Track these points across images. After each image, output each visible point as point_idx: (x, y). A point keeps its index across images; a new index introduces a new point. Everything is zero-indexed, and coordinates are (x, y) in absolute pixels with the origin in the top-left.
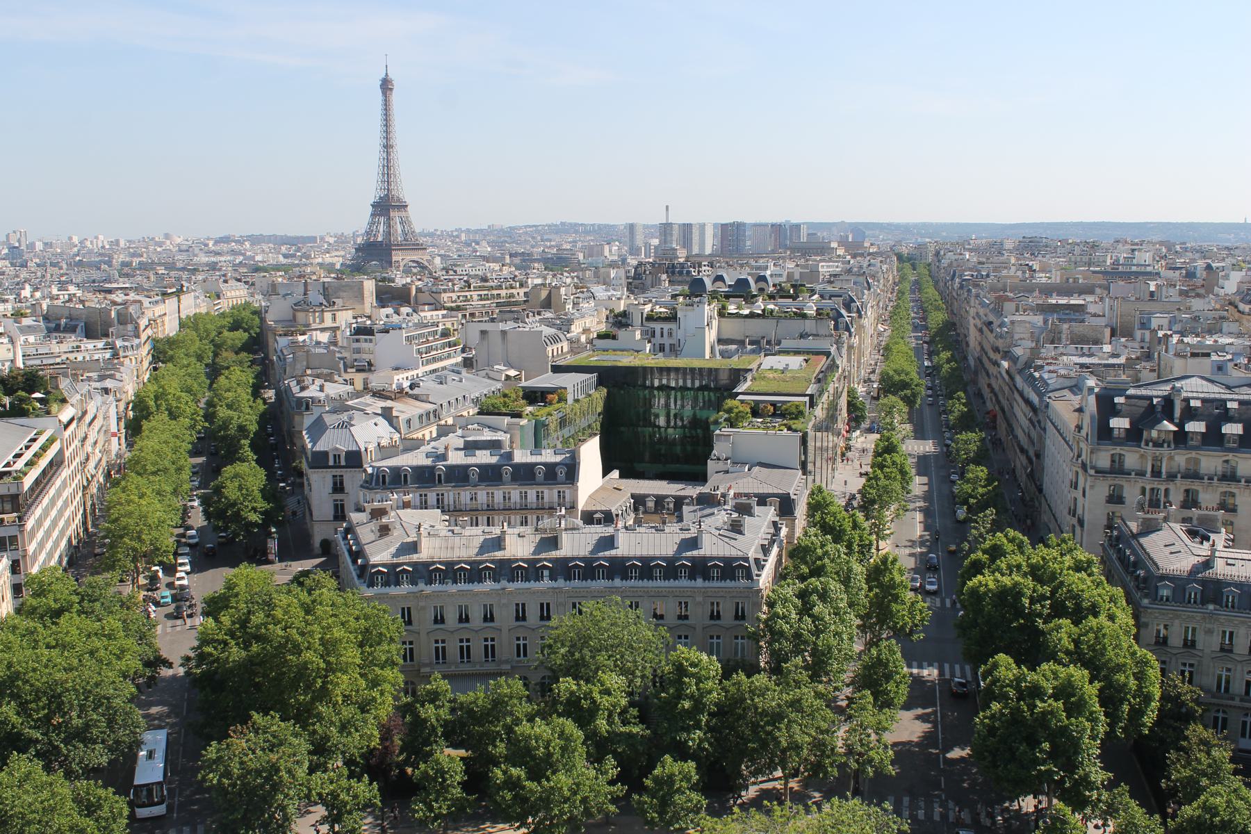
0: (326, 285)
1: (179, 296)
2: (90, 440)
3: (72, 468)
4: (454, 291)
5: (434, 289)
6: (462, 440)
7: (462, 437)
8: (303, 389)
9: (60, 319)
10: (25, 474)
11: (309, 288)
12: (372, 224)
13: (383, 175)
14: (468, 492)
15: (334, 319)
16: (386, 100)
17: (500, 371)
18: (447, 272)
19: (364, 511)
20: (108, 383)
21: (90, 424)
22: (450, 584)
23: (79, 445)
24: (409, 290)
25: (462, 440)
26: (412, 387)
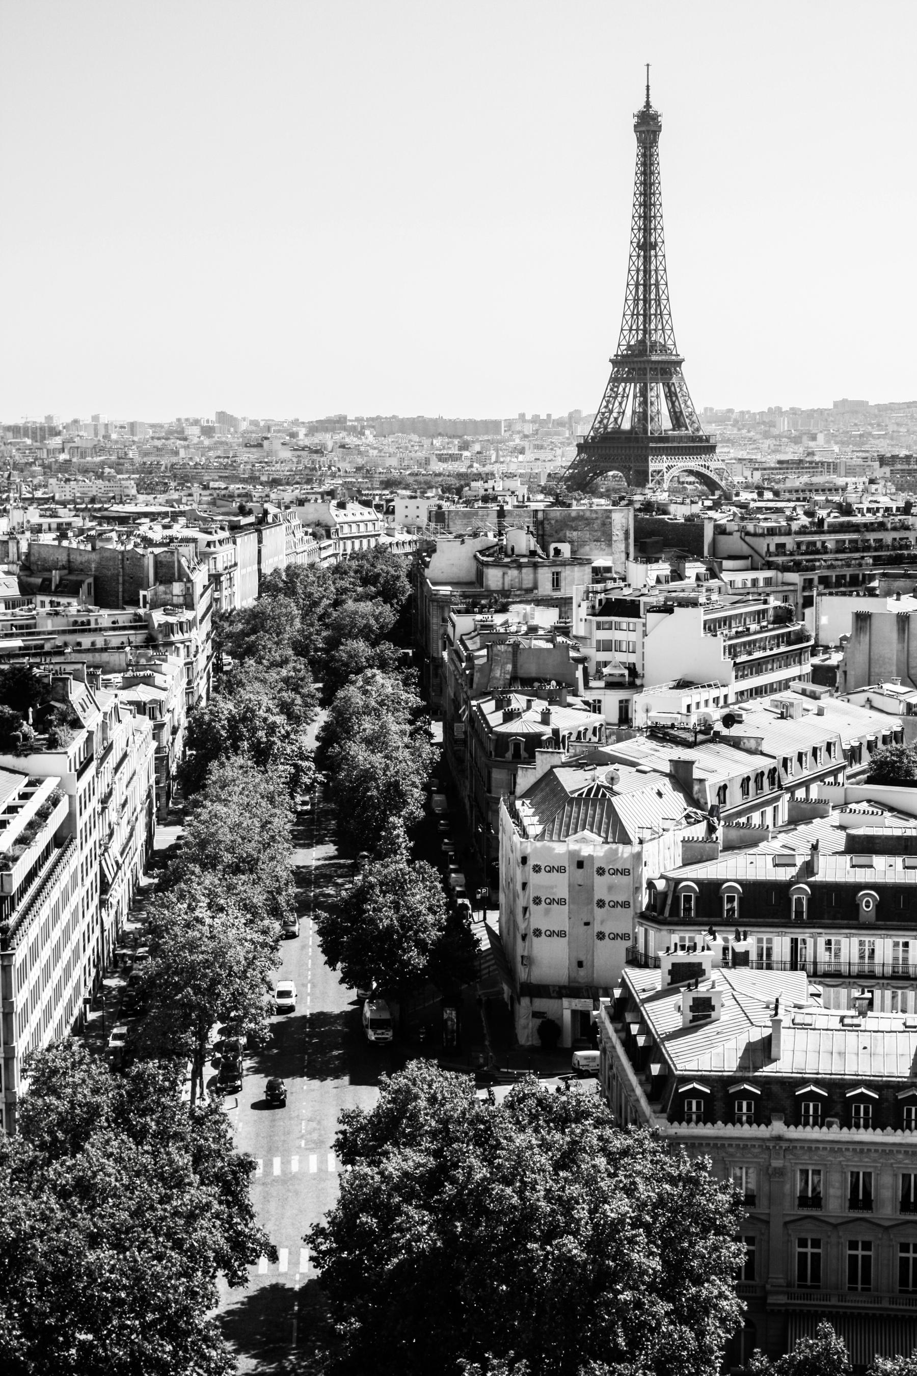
1: (259, 532)
2: (115, 802)
3: (86, 850)
4: (789, 533)
5: (750, 527)
6: (843, 834)
7: (842, 827)
8: (509, 716)
9: (50, 571)
10: (15, 859)
12: (612, 396)
13: (636, 300)
14: (855, 941)
15: (556, 583)
16: (644, 155)
17: (893, 695)
18: (760, 494)
19: (657, 966)
20: (142, 693)
21: (116, 769)
22: (835, 1128)
23: (99, 807)
24: (701, 528)
25: (843, 834)
26: (730, 720)
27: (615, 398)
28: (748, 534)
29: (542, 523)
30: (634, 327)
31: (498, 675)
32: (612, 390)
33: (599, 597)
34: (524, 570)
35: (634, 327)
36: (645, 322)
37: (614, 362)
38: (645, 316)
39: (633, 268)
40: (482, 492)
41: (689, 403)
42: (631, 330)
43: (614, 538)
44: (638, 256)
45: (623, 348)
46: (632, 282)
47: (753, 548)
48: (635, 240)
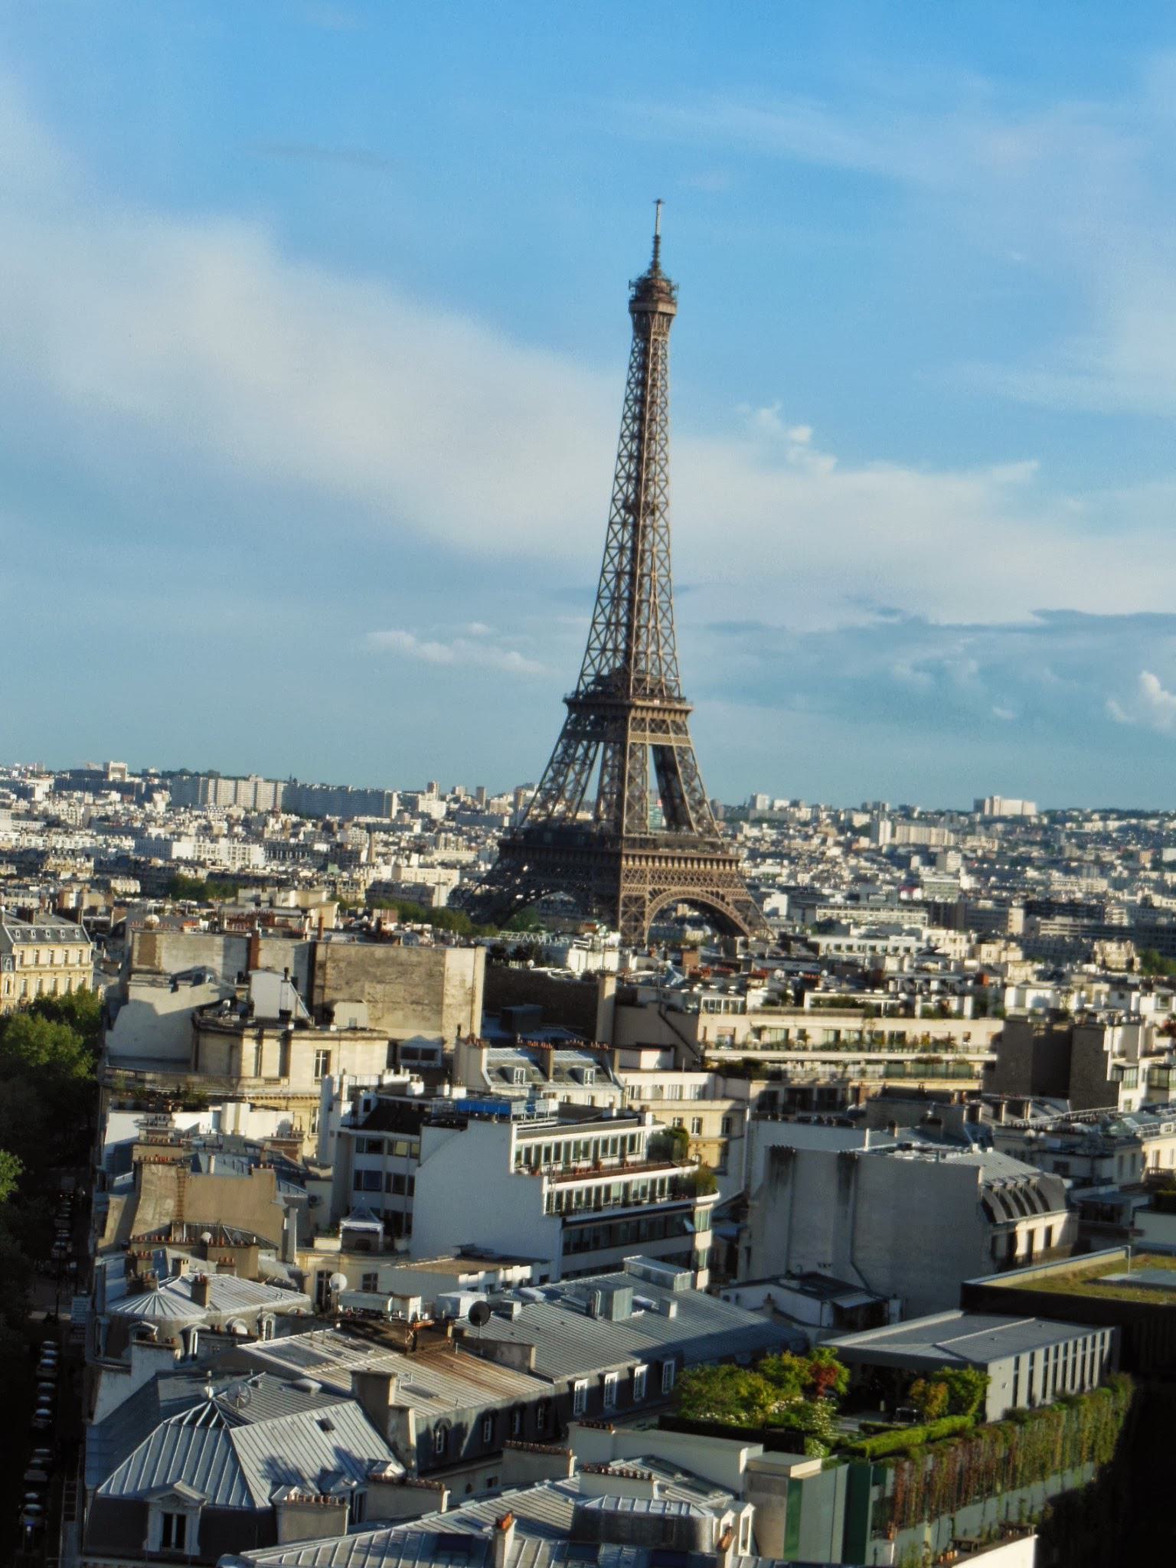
4: (743, 1010)
12: (561, 763)
13: (615, 601)
16: (645, 352)
28: (672, 1008)
30: (610, 645)
31: (149, 1217)
32: (565, 752)
35: (610, 645)
36: (628, 637)
37: (572, 703)
38: (629, 626)
39: (614, 543)
41: (696, 783)
42: (603, 650)
43: (447, 1001)
44: (624, 524)
45: (588, 679)
46: (610, 568)
47: (677, 1033)
48: (620, 496)
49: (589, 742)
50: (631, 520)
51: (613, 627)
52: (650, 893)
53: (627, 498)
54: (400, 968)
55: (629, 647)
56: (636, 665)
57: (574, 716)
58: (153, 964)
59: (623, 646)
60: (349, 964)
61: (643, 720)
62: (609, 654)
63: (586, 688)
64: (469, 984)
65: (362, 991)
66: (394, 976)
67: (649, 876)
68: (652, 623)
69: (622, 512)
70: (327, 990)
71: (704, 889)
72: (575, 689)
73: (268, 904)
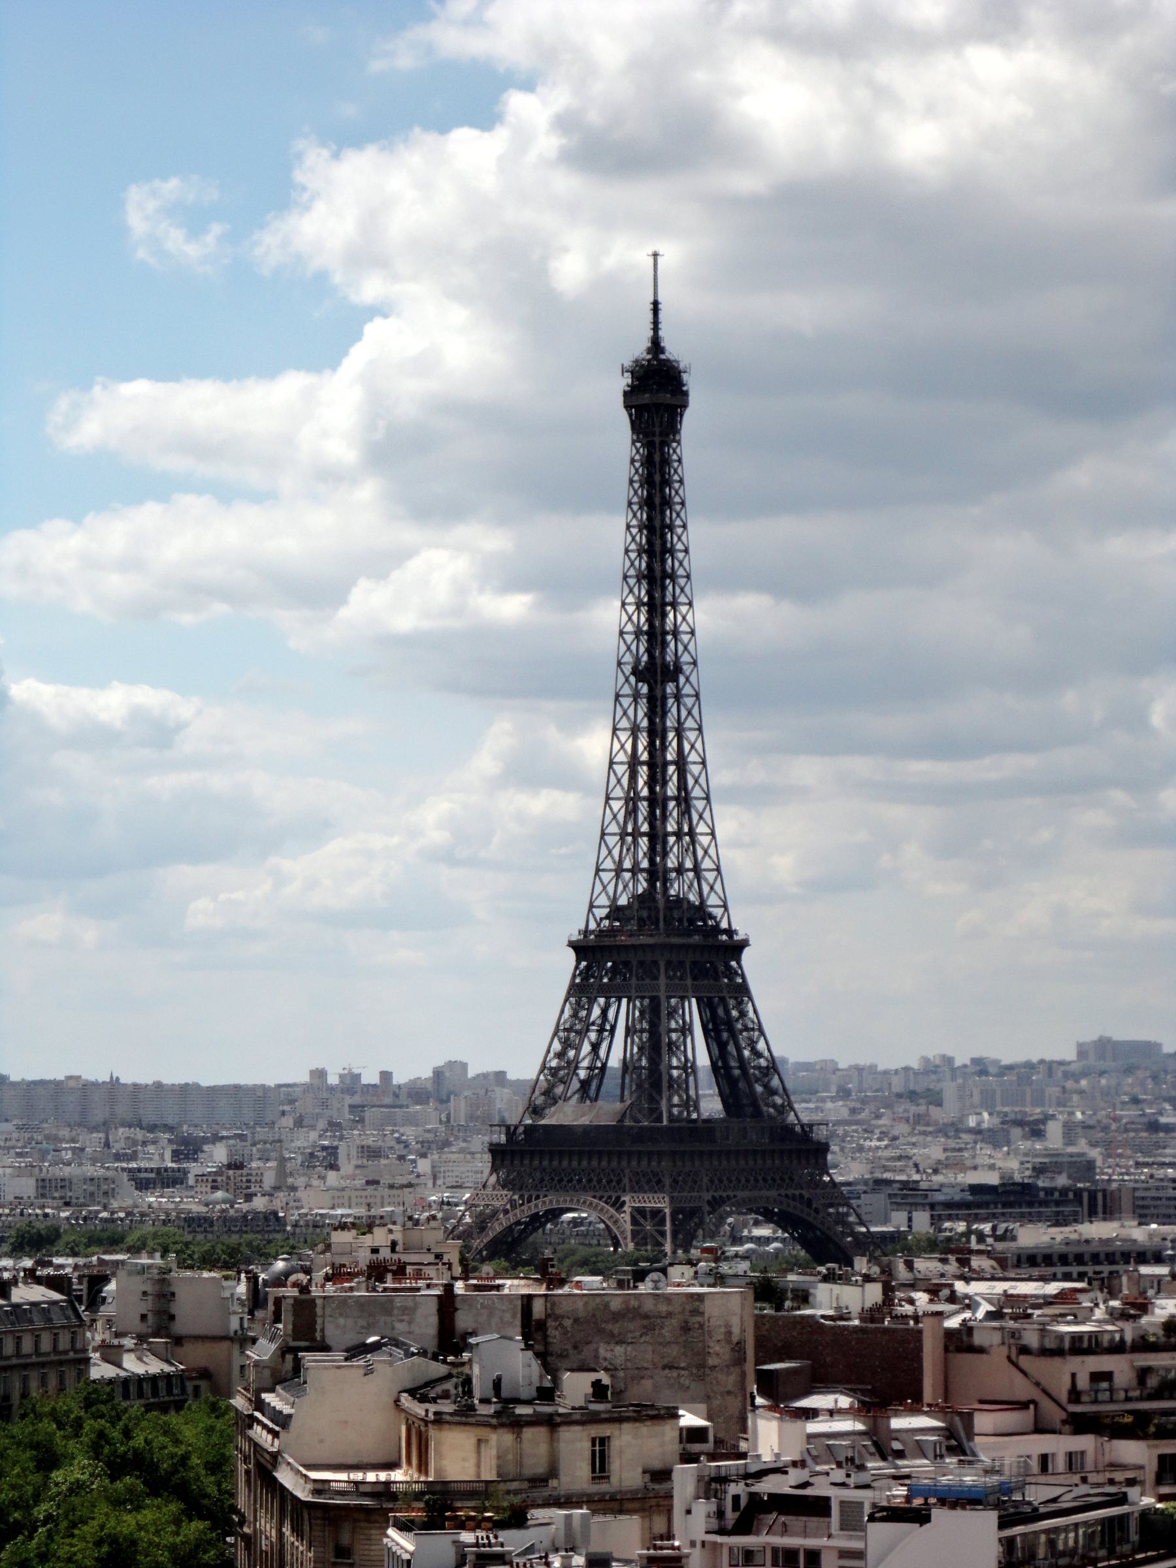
0: (538, 1308)
4: (1118, 1348)
11: (463, 1321)
13: (632, 801)
16: (648, 462)
18: (964, 1262)
27: (583, 1033)
28: (1024, 1350)
29: (541, 1325)
30: (627, 864)
32: (575, 1015)
33: (734, 1489)
34: (528, 1433)
37: (580, 949)
38: (652, 836)
39: (624, 724)
40: (364, 1258)
41: (761, 1046)
42: (619, 870)
43: (711, 1361)
44: (636, 696)
46: (621, 757)
47: (1038, 1384)
48: (628, 658)
49: (608, 998)
50: (644, 689)
51: (629, 839)
52: (709, 1202)
53: (637, 659)
54: (646, 1322)
55: (652, 861)
56: (665, 889)
57: (584, 964)
58: (313, 1339)
59: (645, 864)
60: (576, 1321)
61: (681, 963)
62: (627, 875)
63: (598, 925)
64: (735, 1339)
65: (597, 1357)
66: (638, 1334)
67: (705, 1180)
68: (686, 829)
69: (632, 679)
70: (549, 1359)
71: (783, 1192)
72: (583, 927)
73: (389, 1249)
